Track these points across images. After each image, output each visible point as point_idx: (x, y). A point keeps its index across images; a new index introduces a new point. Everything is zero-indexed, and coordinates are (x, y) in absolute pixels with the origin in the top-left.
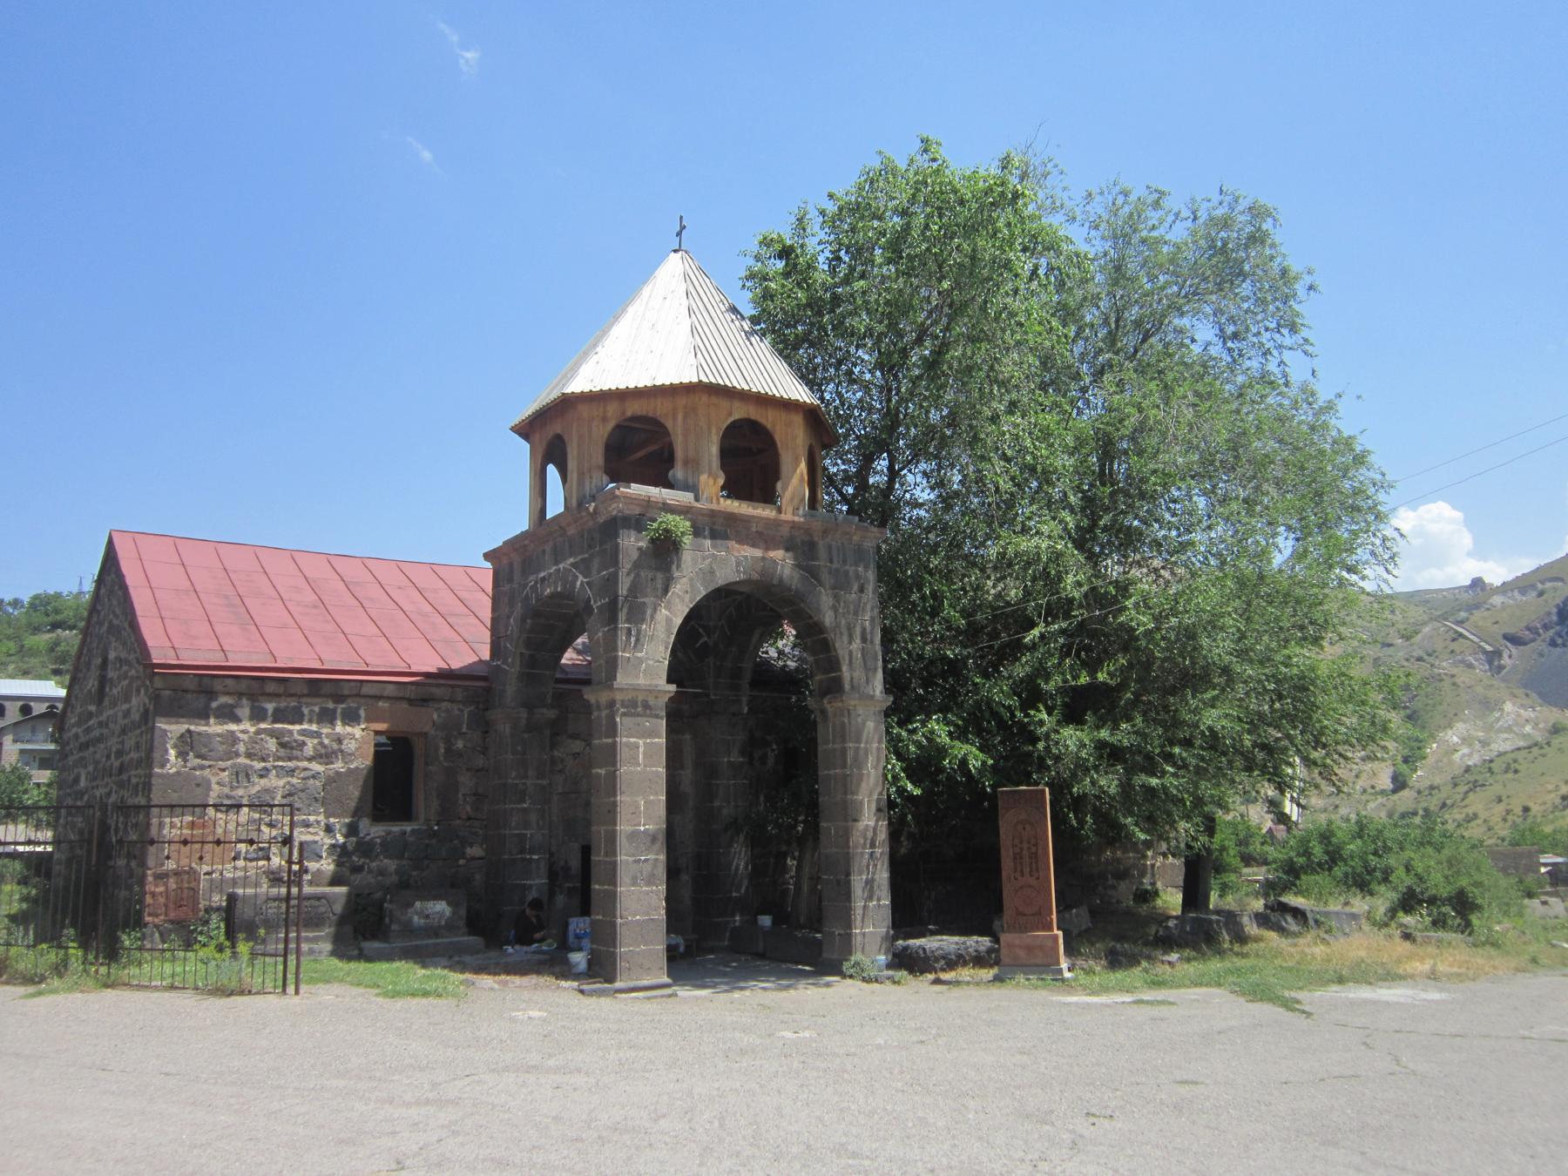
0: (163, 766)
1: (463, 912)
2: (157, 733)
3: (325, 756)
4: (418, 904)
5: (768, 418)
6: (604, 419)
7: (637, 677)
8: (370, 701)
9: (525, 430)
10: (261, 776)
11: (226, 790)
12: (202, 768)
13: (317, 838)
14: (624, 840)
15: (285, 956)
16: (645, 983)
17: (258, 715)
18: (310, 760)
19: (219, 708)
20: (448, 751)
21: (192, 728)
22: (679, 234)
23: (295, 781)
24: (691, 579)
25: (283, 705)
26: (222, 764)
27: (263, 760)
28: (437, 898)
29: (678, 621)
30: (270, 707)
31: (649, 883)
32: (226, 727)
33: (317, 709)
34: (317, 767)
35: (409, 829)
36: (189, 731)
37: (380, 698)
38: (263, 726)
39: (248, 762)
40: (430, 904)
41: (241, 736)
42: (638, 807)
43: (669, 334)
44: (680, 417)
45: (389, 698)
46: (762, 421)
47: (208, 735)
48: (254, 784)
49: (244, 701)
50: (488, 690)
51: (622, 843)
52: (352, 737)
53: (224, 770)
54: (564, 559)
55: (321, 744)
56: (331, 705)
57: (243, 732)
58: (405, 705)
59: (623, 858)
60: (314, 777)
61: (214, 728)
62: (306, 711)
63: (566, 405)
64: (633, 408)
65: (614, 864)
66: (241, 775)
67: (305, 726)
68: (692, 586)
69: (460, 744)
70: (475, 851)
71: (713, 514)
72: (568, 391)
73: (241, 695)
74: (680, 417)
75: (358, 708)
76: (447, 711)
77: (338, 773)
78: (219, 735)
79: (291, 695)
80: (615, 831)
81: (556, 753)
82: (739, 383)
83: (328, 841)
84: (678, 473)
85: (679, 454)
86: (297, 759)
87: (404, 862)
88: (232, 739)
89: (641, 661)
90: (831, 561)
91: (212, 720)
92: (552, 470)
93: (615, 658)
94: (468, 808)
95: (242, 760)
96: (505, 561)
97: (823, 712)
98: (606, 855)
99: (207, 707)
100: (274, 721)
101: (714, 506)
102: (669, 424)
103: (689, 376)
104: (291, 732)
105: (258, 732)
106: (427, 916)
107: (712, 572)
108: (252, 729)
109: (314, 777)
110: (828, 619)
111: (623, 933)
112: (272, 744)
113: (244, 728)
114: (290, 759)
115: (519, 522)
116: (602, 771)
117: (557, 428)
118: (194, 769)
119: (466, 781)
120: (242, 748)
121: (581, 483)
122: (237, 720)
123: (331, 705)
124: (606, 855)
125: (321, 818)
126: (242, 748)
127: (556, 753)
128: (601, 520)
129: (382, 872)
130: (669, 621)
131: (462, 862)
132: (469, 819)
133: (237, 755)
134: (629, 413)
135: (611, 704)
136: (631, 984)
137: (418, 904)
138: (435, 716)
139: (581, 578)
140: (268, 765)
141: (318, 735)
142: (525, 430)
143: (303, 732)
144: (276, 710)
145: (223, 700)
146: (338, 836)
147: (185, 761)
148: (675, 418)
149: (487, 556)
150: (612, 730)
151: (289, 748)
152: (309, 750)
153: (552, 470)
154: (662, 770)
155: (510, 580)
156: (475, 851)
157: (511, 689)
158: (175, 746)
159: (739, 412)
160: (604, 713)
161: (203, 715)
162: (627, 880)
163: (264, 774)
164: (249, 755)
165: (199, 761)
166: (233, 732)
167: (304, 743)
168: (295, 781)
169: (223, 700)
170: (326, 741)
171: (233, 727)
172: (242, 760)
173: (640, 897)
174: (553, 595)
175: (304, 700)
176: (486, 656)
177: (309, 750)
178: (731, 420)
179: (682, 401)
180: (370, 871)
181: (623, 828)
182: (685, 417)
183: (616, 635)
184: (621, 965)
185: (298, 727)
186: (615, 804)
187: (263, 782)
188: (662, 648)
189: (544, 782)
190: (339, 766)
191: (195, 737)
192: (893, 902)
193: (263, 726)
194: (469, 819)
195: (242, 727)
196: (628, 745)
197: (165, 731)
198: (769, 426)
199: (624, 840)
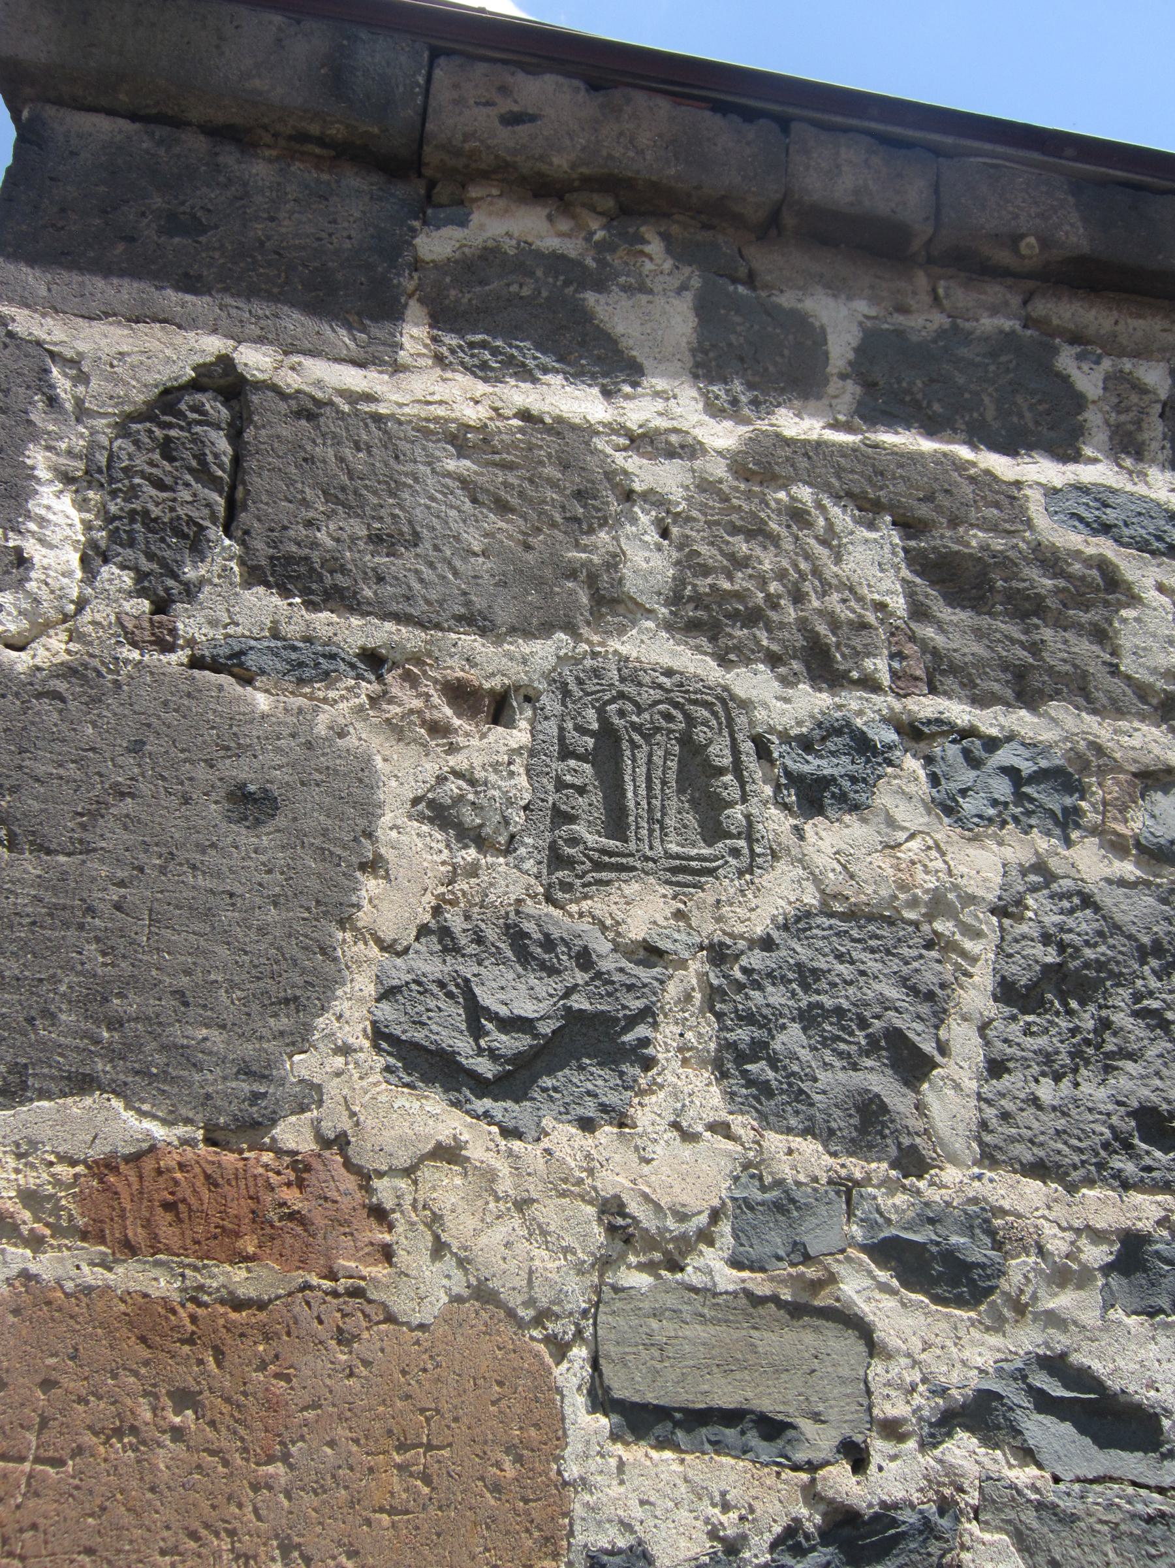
10: (811, 797)
11: (509, 881)
12: (309, 665)
17: (749, 356)
19: (478, 265)
21: (255, 360)
23: (1088, 862)
25: (924, 322)
30: (842, 321)
41: (645, 473)
53: (498, 708)
57: (643, 441)
61: (427, 385)
66: (642, 775)
78: (460, 438)
86: (1078, 688)
88: (569, 486)
91: (414, 336)
95: (651, 647)
99: (393, 249)
100: (881, 406)
104: (1008, 496)
105: (761, 465)
108: (722, 437)
112: (872, 564)
113: (668, 422)
114: (1026, 690)
118: (234, 664)
120: (646, 561)
122: (613, 366)
133: (610, 602)
140: (867, 711)
144: (874, 349)
145: (505, 225)
161: (358, 296)
164: (704, 615)
165: (262, 607)
172: (651, 647)
187: (827, 838)
191: (272, 428)
193: (797, 424)
195: (639, 412)
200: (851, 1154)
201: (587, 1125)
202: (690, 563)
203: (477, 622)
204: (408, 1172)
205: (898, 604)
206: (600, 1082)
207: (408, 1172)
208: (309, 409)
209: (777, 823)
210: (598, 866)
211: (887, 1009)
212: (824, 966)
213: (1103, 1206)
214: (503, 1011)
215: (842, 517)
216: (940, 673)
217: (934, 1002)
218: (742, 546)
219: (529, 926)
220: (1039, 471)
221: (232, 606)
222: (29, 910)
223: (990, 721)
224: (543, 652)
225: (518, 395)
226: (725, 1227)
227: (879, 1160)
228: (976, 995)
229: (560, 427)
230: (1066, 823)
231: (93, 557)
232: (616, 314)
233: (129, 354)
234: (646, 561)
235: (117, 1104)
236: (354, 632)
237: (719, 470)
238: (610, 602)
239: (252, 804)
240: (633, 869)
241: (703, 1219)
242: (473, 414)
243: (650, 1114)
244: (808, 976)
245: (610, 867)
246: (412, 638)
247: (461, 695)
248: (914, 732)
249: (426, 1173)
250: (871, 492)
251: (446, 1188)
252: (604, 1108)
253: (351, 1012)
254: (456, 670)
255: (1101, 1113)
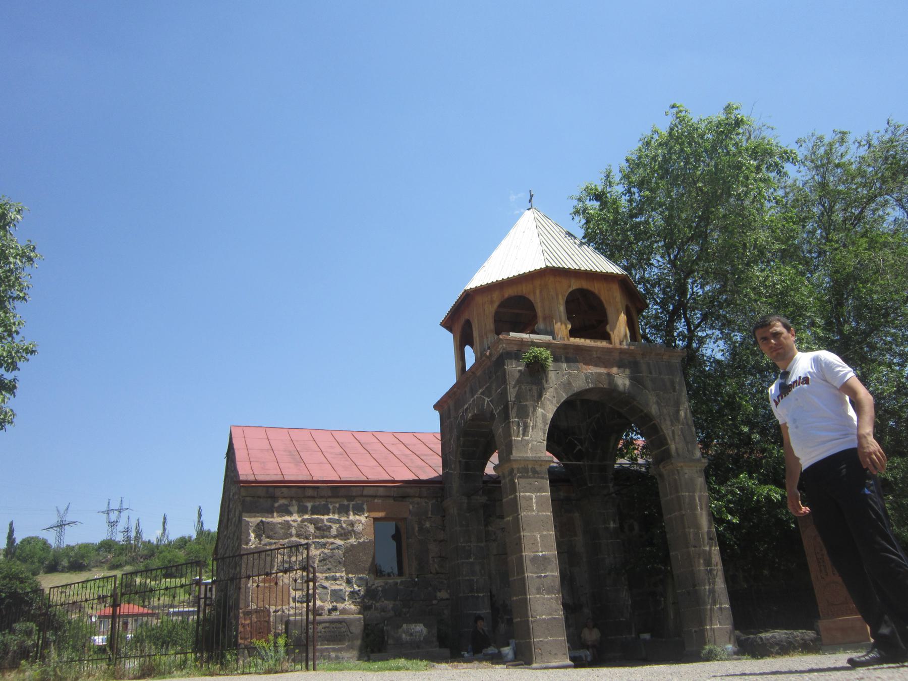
0: (247, 544)
1: (435, 631)
2: (243, 524)
3: (344, 534)
4: (405, 625)
5: (595, 287)
6: (492, 302)
7: (527, 453)
8: (370, 499)
9: (448, 323)
12: (271, 544)
13: (342, 588)
14: (529, 563)
15: (307, 645)
16: (554, 664)
17: (302, 511)
18: (335, 537)
19: (280, 506)
20: (421, 529)
21: (264, 519)
22: (530, 201)
23: (326, 551)
24: (556, 389)
25: (317, 503)
27: (307, 538)
28: (416, 621)
29: (550, 416)
31: (548, 594)
32: (284, 518)
33: (337, 505)
34: (339, 542)
35: (399, 581)
36: (262, 521)
37: (375, 497)
38: (306, 517)
39: (297, 539)
40: (413, 626)
42: (536, 539)
43: (528, 246)
44: (538, 292)
45: (381, 497)
46: (591, 288)
49: (294, 502)
50: (442, 489)
51: (527, 564)
52: (360, 522)
54: (477, 391)
55: (341, 527)
56: (346, 503)
57: (294, 521)
58: (391, 501)
59: (529, 574)
60: (338, 548)
61: (277, 519)
62: (331, 507)
63: (468, 298)
64: (509, 292)
65: (524, 579)
67: (331, 516)
68: (557, 393)
69: (428, 525)
70: (443, 594)
71: (566, 347)
72: (468, 288)
73: (292, 498)
74: (538, 292)
75: (363, 504)
76: (418, 503)
77: (352, 545)
78: (280, 523)
79: (322, 497)
80: (522, 556)
81: (490, 528)
82: (572, 266)
83: (348, 589)
84: (541, 325)
85: (540, 313)
86: (327, 537)
87: (397, 603)
88: (287, 525)
89: (528, 442)
90: (651, 373)
91: (275, 514)
92: (468, 350)
93: (511, 441)
94: (436, 566)
95: (294, 539)
96: (446, 407)
97: (661, 475)
98: (518, 574)
99: (273, 506)
100: (313, 514)
101: (566, 342)
102: (531, 298)
103: (539, 264)
104: (322, 520)
105: (303, 521)
106: (411, 634)
107: (569, 383)
108: (299, 519)
109: (338, 548)
110: (654, 409)
111: (535, 628)
112: (311, 528)
113: (295, 518)
114: (323, 537)
115: (448, 379)
116: (510, 518)
117: (466, 316)
118: (266, 545)
119: (433, 548)
120: (293, 531)
121: (481, 342)
122: (290, 513)
123: (346, 503)
124: (518, 574)
125: (343, 574)
126: (293, 531)
127: (490, 528)
128: (494, 359)
129: (383, 610)
130: (544, 416)
131: (435, 602)
132: (437, 573)
133: (291, 536)
134: (506, 296)
135: (512, 471)
136: (544, 665)
137: (405, 625)
138: (411, 507)
139: (487, 399)
140: (310, 541)
141: (339, 521)
142: (448, 323)
143: (329, 520)
144: (313, 507)
146: (355, 586)
147: (260, 540)
148: (535, 293)
149: (436, 407)
150: (514, 489)
151: (322, 530)
152: (334, 532)
153: (468, 350)
154: (550, 514)
155: (449, 417)
156: (443, 594)
157: (455, 484)
158: (254, 531)
159: (575, 285)
160: (507, 480)
161: (270, 511)
162: (533, 590)
164: (298, 536)
165: (267, 540)
166: (288, 521)
167: (331, 527)
168: (326, 551)
169: (281, 502)
170: (344, 525)
171: (288, 518)
173: (544, 605)
174: (475, 418)
175: (330, 500)
176: (440, 471)
177: (334, 532)
178: (571, 290)
179: (537, 283)
180: (376, 609)
181: (527, 554)
182: (541, 292)
183: (509, 427)
184: (536, 651)
185: (326, 517)
186: (520, 538)
188: (541, 434)
189: (483, 545)
190: (353, 541)
192: (731, 605)
193: (306, 517)
194: (437, 573)
195: (293, 518)
196: (524, 497)
197: (248, 522)
198: (596, 292)
199: (529, 563)
208: (268, 523)
213: (324, 575)
216: (316, 537)
228: (317, 562)
232: (291, 509)
236: (273, 541)
250: (311, 521)
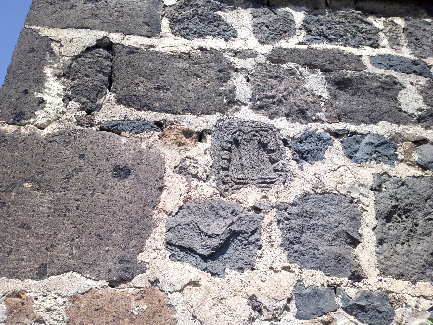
0: (19, 118)
11: (207, 190)
12: (139, 127)
21: (115, 37)
23: (402, 171)
26: (197, 123)
47: (151, 54)
48: (286, 177)
53: (201, 137)
95: (246, 114)
105: (277, 58)
108: (264, 50)
112: (316, 83)
118: (113, 128)
120: (243, 89)
133: (233, 102)
158: (65, 74)
163: (307, 151)
191: (121, 57)
195: (236, 45)
200: (334, 275)
201: (241, 269)
202: (258, 89)
203: (192, 111)
204: (181, 291)
205: (326, 95)
206: (244, 255)
207: (181, 291)
208: (133, 51)
209: (293, 166)
210: (237, 183)
211: (339, 224)
212: (316, 211)
214: (209, 233)
215: (304, 71)
217: (356, 219)
218: (273, 82)
219: (215, 204)
220: (366, 52)
221: (111, 110)
222: (47, 211)
223: (362, 129)
224: (213, 119)
225: (199, 42)
226: (292, 305)
227: (344, 277)
228: (369, 219)
229: (213, 51)
230: (392, 159)
231: (67, 99)
233: (76, 38)
234: (243, 89)
235: (78, 275)
236: (150, 116)
237: (263, 60)
238: (233, 102)
239: (122, 172)
240: (248, 183)
241: (285, 302)
242: (185, 49)
243: (262, 265)
244: (311, 215)
245: (241, 183)
246: (169, 117)
247: (188, 134)
248: (337, 134)
249: (187, 290)
251: (194, 295)
252: (246, 264)
253: (157, 238)
254: (185, 126)
255: (419, 255)
